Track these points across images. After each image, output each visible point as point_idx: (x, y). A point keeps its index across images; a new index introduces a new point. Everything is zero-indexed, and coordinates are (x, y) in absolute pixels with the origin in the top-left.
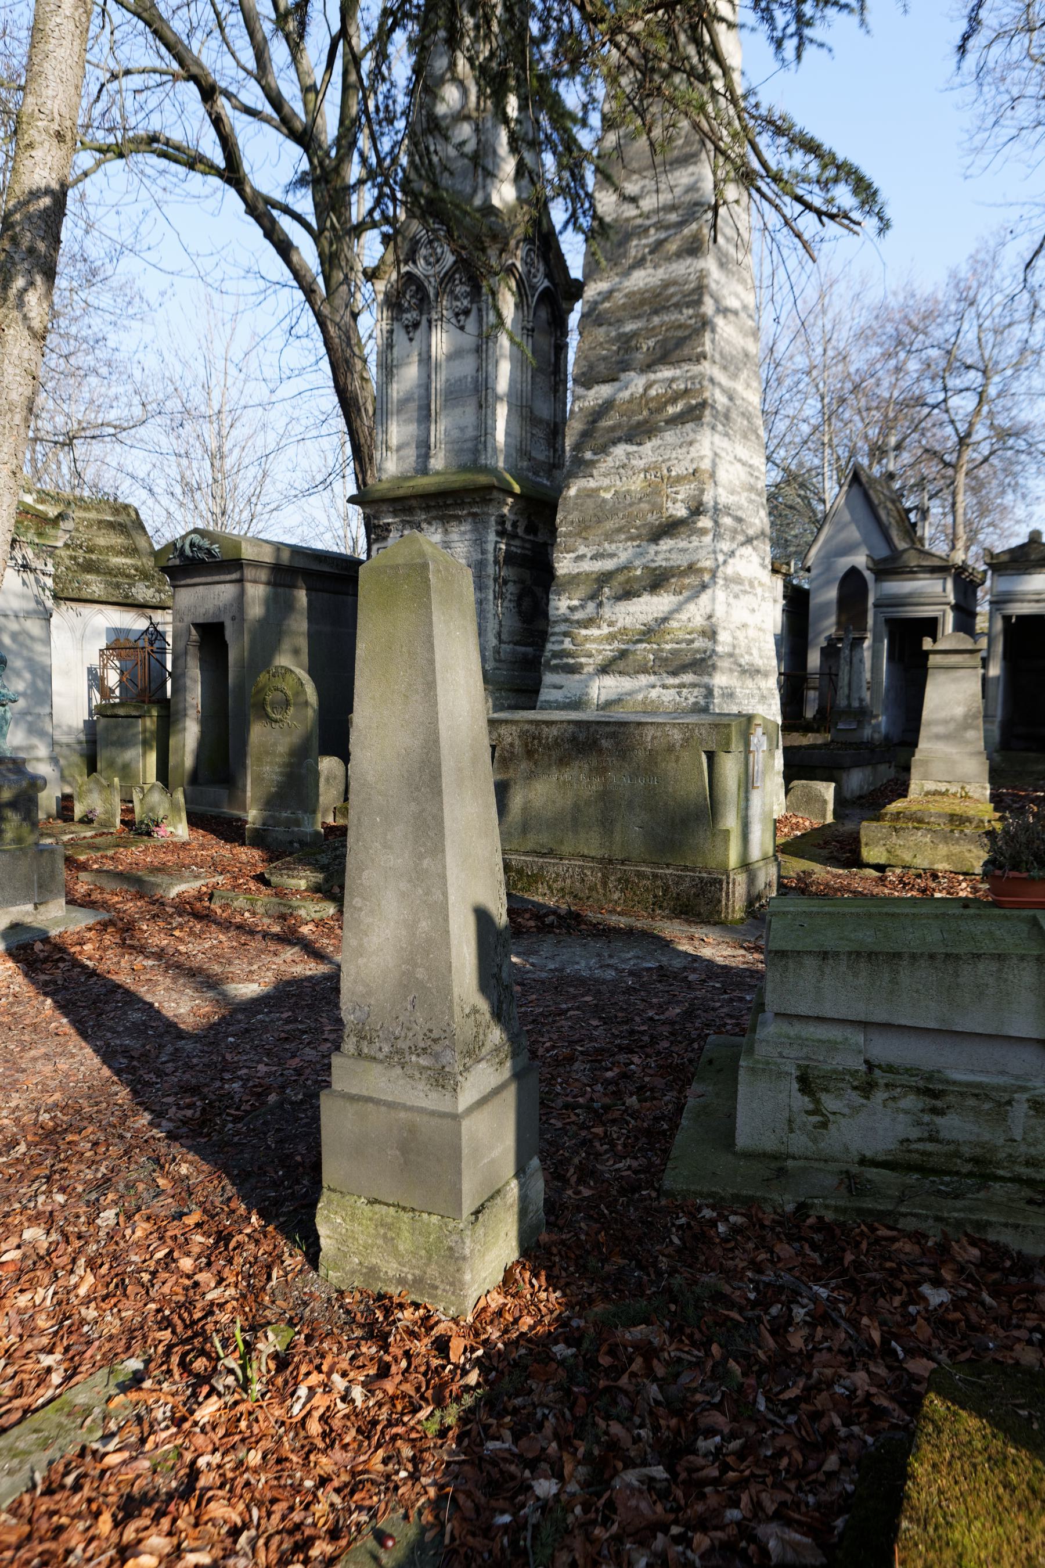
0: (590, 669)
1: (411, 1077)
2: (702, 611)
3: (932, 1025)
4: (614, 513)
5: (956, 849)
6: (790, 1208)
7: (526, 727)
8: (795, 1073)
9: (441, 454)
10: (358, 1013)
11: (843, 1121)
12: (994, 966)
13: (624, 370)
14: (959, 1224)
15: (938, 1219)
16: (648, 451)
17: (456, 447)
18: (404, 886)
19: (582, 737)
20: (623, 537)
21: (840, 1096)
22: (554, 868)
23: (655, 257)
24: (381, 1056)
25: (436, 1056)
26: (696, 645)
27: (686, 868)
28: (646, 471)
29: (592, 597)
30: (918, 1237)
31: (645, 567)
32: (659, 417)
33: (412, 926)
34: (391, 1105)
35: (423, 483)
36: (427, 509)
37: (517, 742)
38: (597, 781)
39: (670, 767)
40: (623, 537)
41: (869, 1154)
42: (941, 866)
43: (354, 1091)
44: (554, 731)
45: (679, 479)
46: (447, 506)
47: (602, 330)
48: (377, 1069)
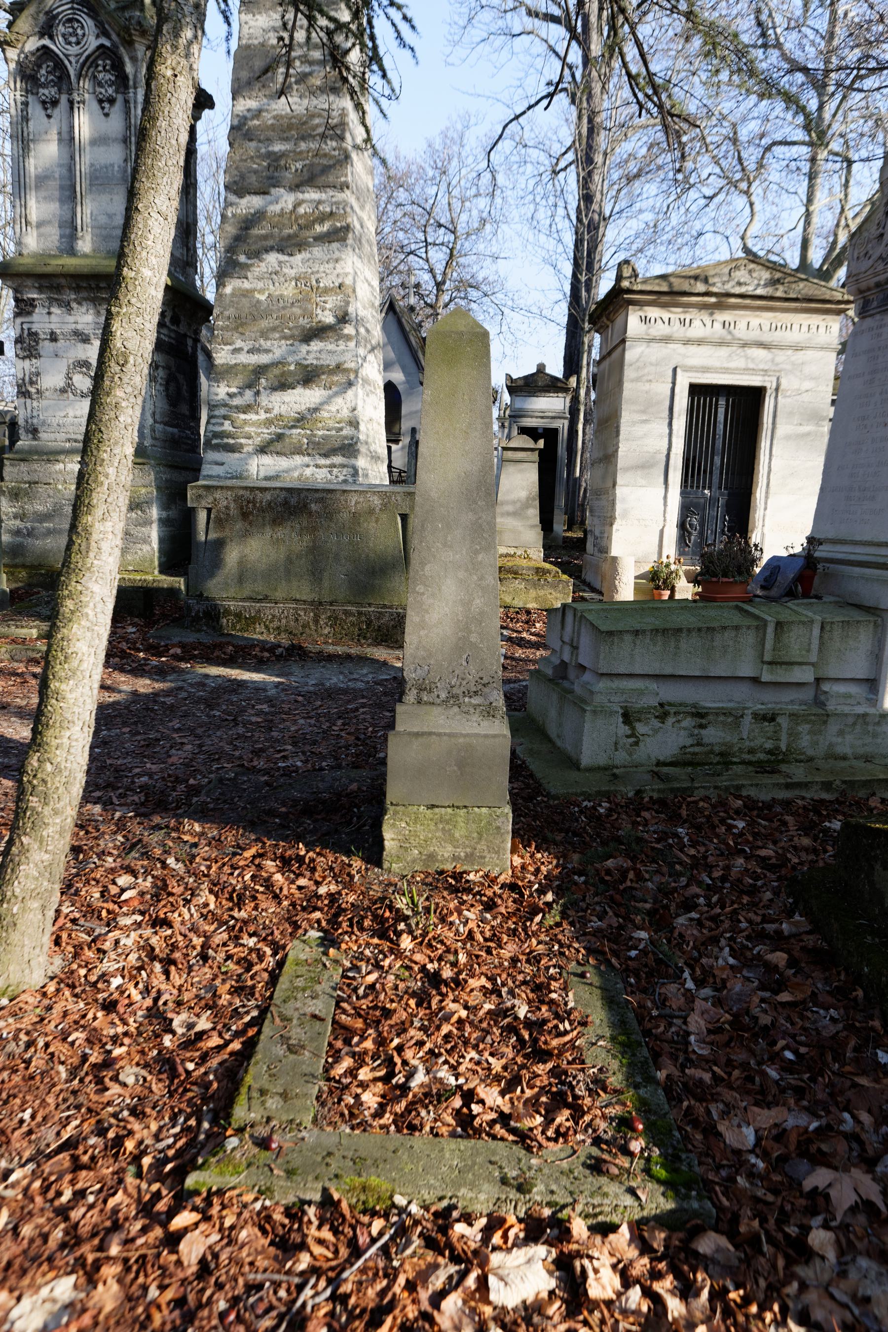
0: (250, 449)
1: (467, 713)
2: (349, 405)
3: (697, 674)
4: (267, 314)
5: (542, 593)
6: (631, 794)
7: (241, 492)
8: (621, 711)
9: (88, 238)
10: (419, 671)
11: (648, 740)
12: (733, 634)
13: (274, 186)
14: (727, 789)
15: (716, 787)
16: (298, 262)
17: (104, 232)
18: (461, 574)
19: (293, 501)
20: (277, 335)
21: (647, 724)
22: (269, 610)
23: (302, 87)
24: (438, 701)
25: (485, 697)
26: (344, 432)
27: (385, 606)
28: (297, 280)
29: (249, 386)
30: (706, 799)
31: (298, 364)
32: (308, 234)
33: (467, 604)
34: (450, 735)
35: (70, 263)
36: (77, 289)
37: (232, 505)
38: (307, 538)
39: (370, 526)
40: (277, 335)
41: (662, 759)
42: (531, 606)
43: (415, 730)
44: (268, 496)
45: (326, 291)
46: (99, 289)
47: (253, 144)
48: (436, 710)
